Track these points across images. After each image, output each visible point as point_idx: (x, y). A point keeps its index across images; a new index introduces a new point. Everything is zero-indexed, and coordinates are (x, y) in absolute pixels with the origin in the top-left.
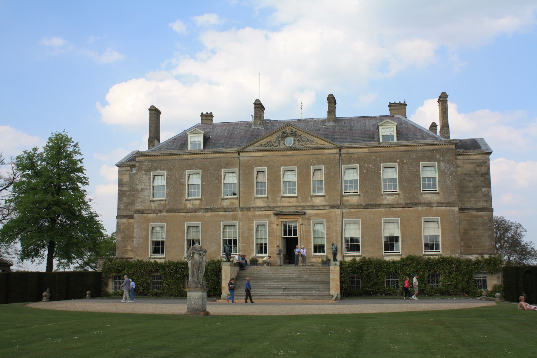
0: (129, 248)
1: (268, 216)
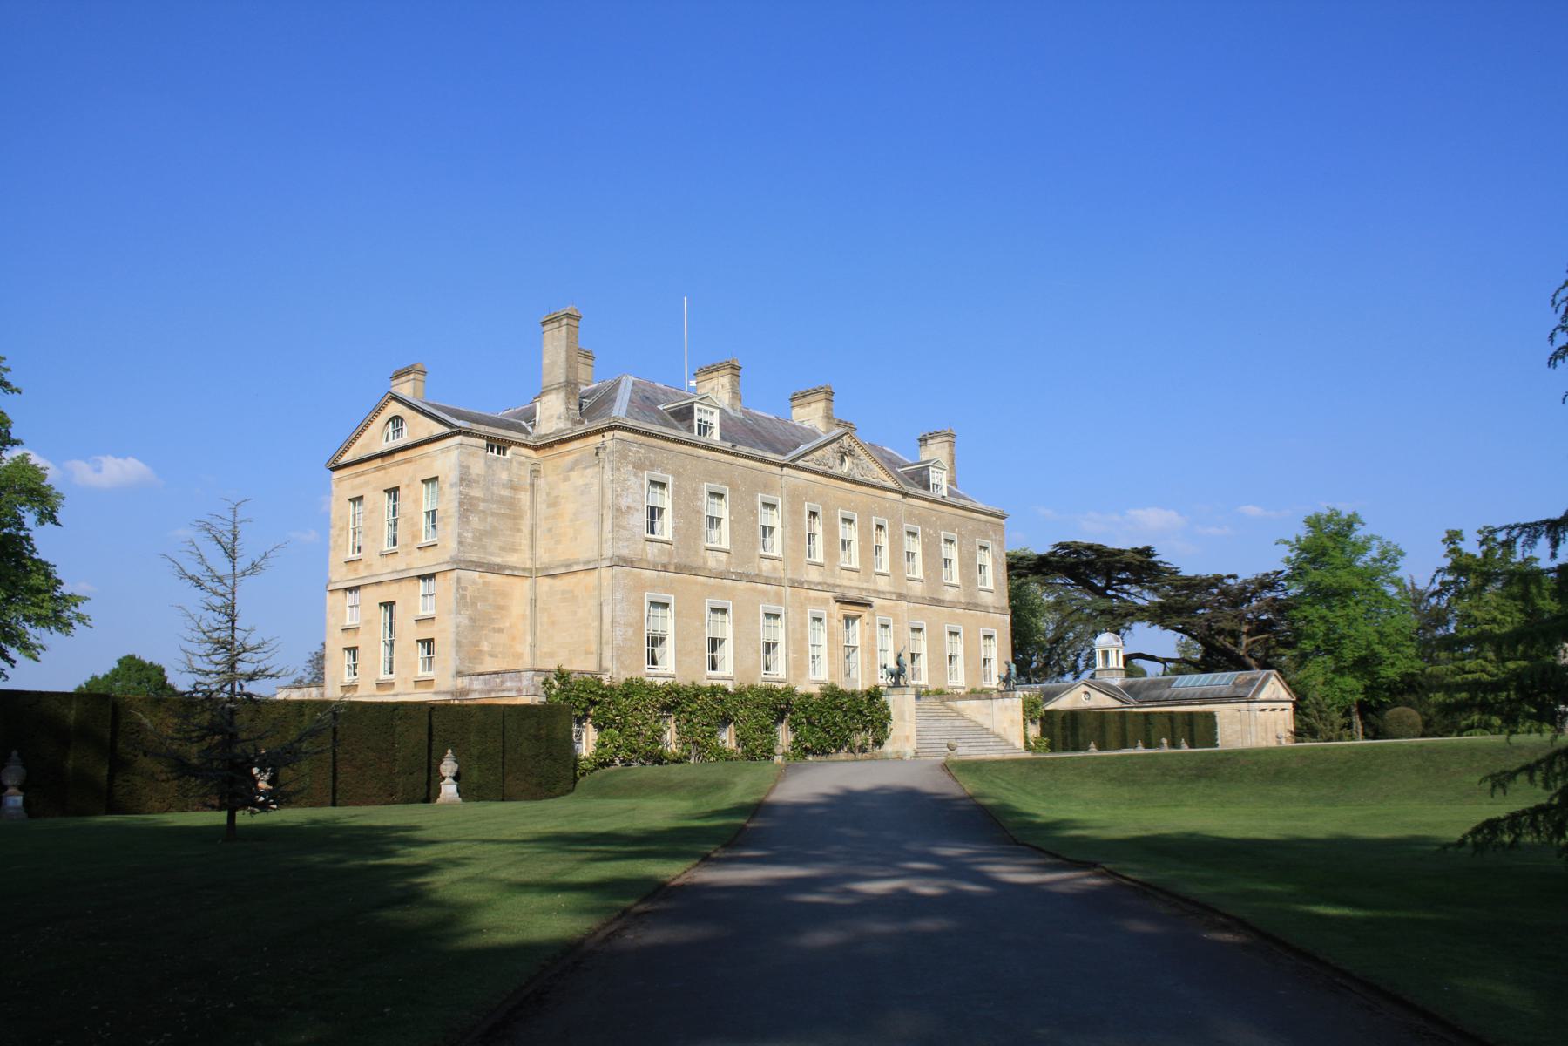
0: (485, 647)
1: (825, 602)
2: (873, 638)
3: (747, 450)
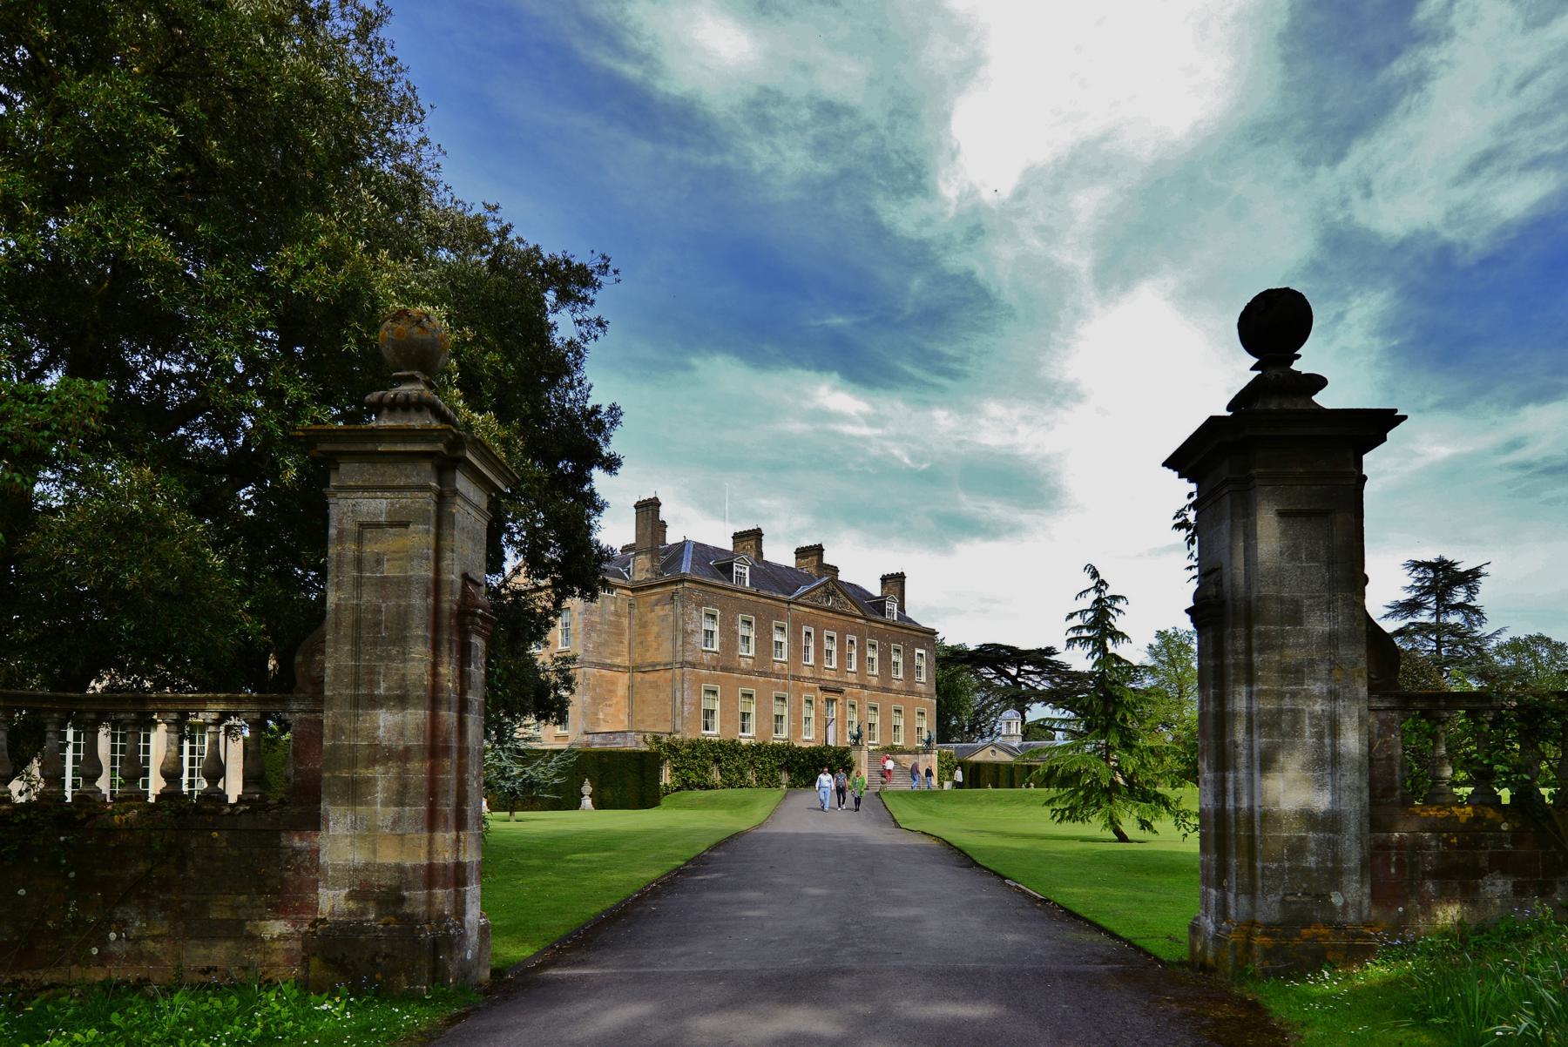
0: (601, 716)
2: (844, 713)
3: (766, 593)
